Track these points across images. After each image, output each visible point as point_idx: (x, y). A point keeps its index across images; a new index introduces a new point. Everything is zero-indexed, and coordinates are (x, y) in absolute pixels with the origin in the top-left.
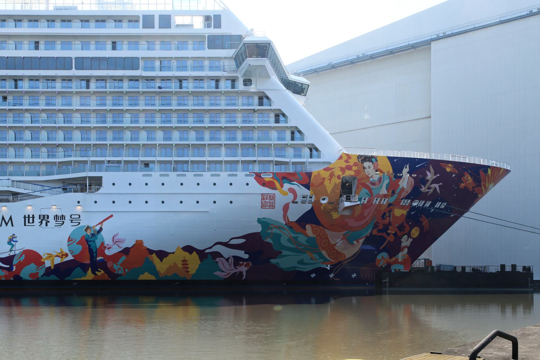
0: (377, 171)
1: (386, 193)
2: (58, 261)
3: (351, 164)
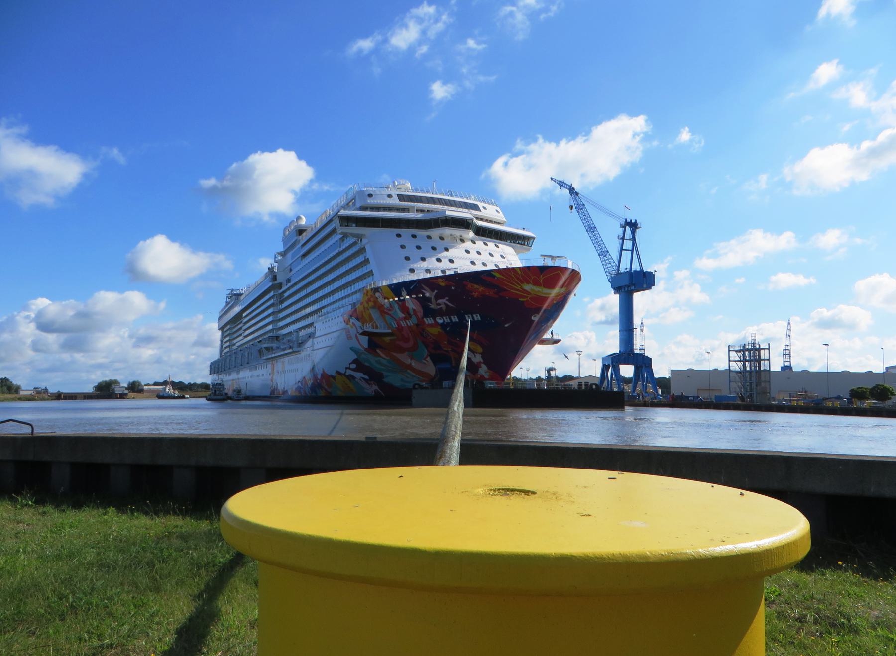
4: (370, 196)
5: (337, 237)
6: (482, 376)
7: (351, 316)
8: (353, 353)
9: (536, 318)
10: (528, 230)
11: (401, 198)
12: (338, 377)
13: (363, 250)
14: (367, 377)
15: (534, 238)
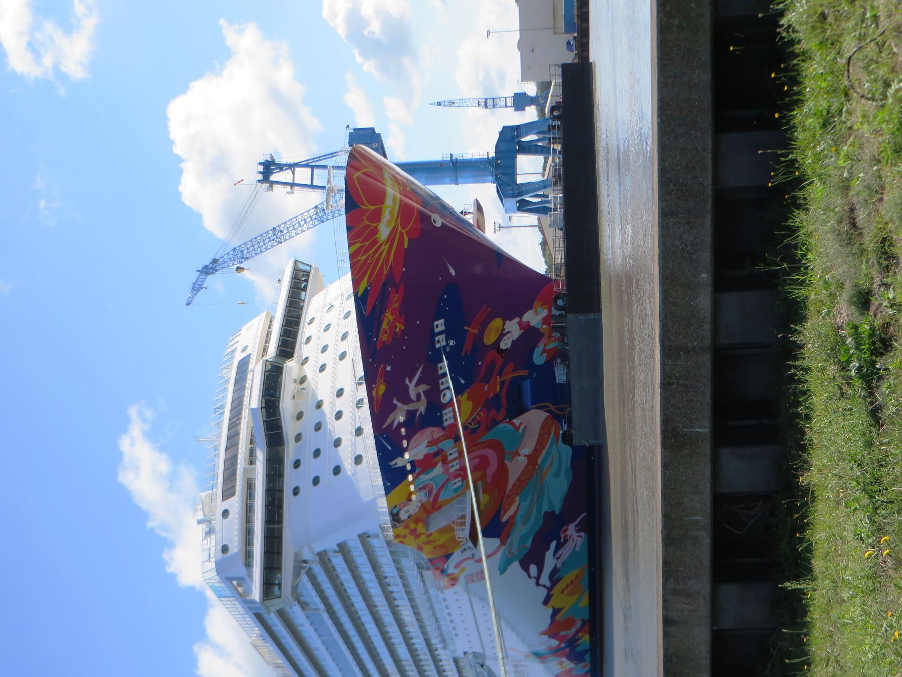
0: (410, 500)
1: (440, 464)
2: (569, 663)
3: (407, 531)
4: (225, 549)
5: (297, 615)
6: (545, 321)
7: (443, 571)
8: (510, 568)
9: (439, 222)
10: (282, 272)
11: (228, 493)
12: (555, 602)
13: (323, 557)
14: (553, 545)
15: (296, 261)
